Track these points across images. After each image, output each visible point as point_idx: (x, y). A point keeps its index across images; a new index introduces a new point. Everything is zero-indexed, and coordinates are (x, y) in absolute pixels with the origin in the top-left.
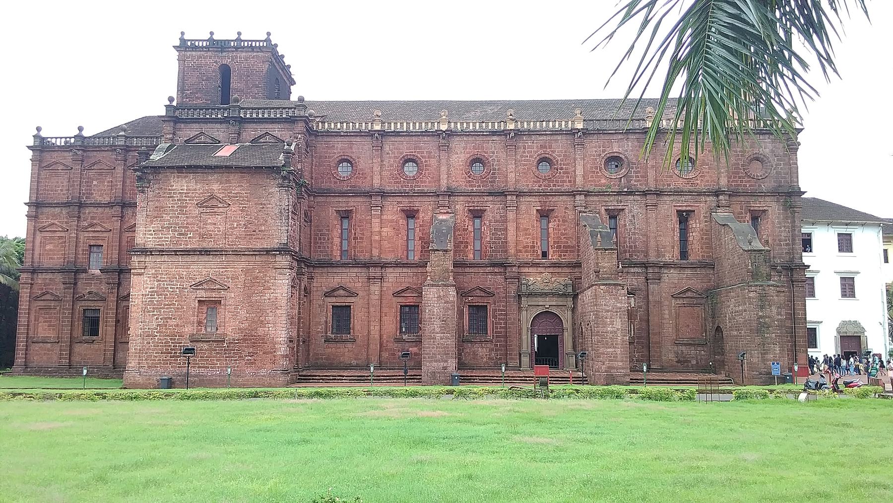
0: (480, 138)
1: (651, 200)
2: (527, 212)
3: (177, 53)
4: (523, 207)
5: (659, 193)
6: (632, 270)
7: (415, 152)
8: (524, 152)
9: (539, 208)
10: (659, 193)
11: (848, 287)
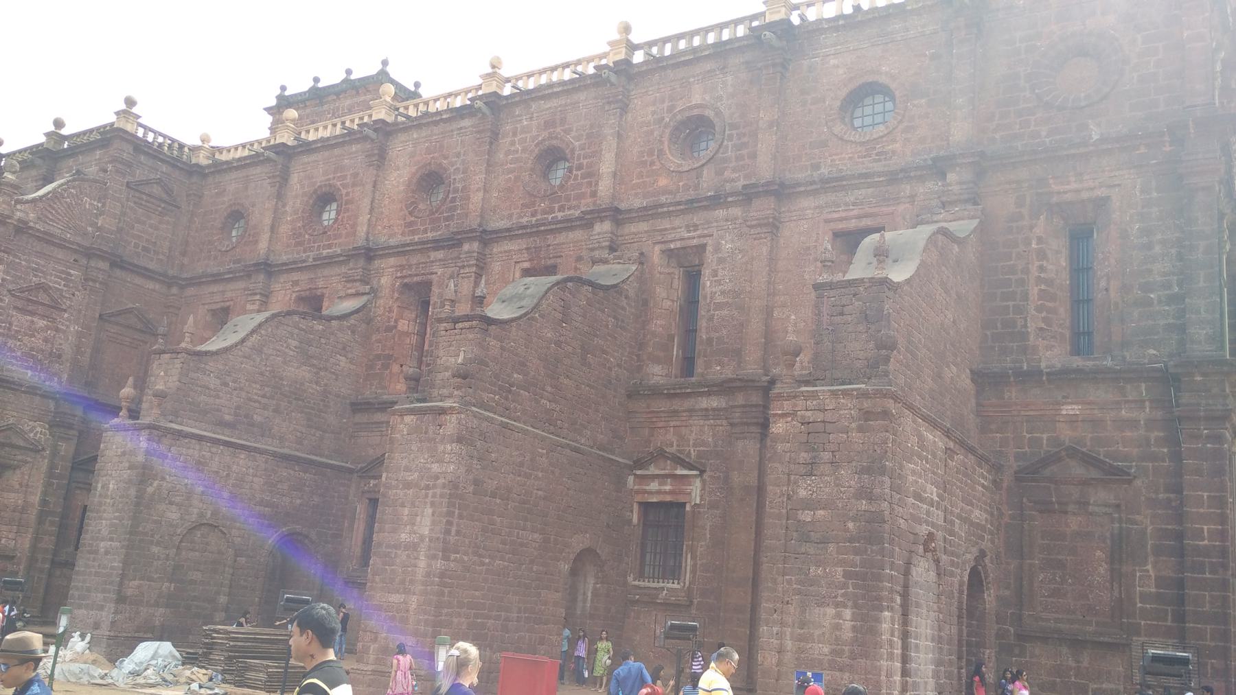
1: (763, 208)
3: (269, 119)
6: (704, 403)
7: (334, 178)
8: (513, 143)
9: (526, 265)
10: (780, 191)
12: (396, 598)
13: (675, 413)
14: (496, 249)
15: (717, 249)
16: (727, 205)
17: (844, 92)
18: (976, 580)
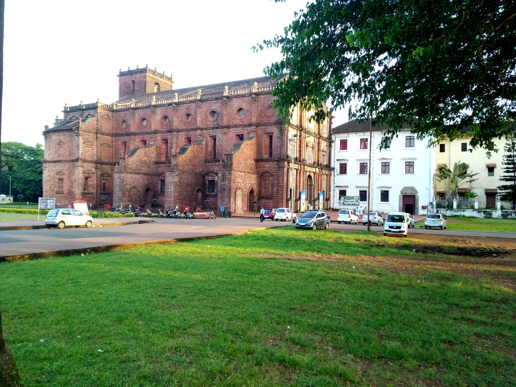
0: (165, 107)
1: (226, 130)
2: (181, 139)
4: (180, 137)
5: (228, 127)
10: (228, 127)
11: (410, 166)
12: (169, 199)
13: (212, 165)
14: (180, 133)
15: (218, 136)
16: (219, 128)
17: (237, 110)
18: (252, 192)
